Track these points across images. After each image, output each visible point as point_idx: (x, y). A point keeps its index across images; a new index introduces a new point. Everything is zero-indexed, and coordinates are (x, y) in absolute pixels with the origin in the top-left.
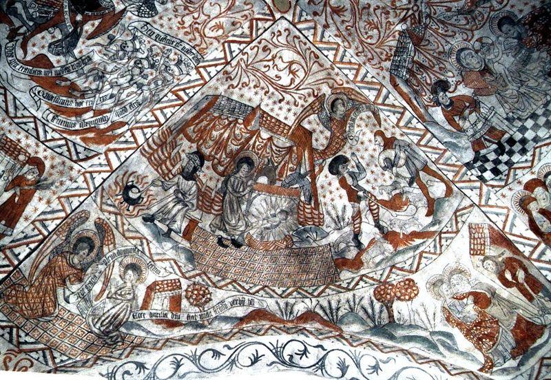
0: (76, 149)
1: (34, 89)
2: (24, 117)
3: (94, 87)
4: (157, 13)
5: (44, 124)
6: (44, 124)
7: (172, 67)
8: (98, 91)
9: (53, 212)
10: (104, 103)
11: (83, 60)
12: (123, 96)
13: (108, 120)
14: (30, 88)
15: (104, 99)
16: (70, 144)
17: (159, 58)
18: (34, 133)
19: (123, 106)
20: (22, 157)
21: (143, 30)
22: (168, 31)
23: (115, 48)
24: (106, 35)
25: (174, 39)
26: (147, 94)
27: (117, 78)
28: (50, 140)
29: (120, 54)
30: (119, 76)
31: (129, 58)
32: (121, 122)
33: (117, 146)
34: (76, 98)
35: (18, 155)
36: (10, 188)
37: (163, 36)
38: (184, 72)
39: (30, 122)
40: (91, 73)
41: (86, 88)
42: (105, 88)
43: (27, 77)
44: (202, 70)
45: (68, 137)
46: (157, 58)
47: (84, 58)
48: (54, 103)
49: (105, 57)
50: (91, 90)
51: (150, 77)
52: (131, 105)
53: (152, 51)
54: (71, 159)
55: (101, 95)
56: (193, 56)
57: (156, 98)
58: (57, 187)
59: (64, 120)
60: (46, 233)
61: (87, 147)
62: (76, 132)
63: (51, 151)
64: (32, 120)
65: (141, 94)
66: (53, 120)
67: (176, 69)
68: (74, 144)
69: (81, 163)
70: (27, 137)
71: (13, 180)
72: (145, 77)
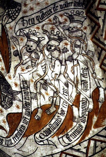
1: (37, 140)
3: (51, 94)
4: (20, 5)
5: (71, 148)
6: (71, 148)
7: (71, 25)
8: (56, 92)
10: (70, 94)
11: (24, 88)
12: (72, 77)
13: (87, 99)
14: (35, 142)
15: (67, 92)
16: (96, 138)
17: (56, 30)
19: (80, 81)
21: (26, 25)
22: (37, 9)
23: (26, 57)
24: (13, 56)
25: (49, 8)
26: (81, 58)
27: (53, 72)
29: (34, 57)
30: (52, 69)
31: (42, 52)
32: (94, 91)
34: (56, 112)
37: (40, 14)
38: (83, 20)
40: (38, 88)
41: (50, 100)
42: (56, 86)
43: (24, 139)
44: (100, 6)
45: (89, 136)
46: (55, 31)
47: (22, 86)
48: (55, 131)
49: (29, 70)
50: (53, 97)
51: (68, 47)
52: (83, 75)
53: (46, 31)
55: (62, 91)
56: (73, 4)
57: (91, 54)
59: (73, 131)
61: (104, 127)
62: (88, 128)
65: (78, 63)
66: (71, 141)
67: (75, 24)
72: (65, 50)
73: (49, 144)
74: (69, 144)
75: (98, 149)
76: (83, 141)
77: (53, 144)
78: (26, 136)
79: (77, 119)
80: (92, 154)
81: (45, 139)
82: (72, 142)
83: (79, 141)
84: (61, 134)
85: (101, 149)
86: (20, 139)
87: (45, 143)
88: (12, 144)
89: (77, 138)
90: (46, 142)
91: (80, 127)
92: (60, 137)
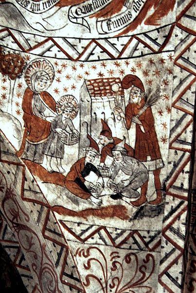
0: (150, 39)
1: (71, 14)
2: (86, 49)
6: (106, 39)
9: (179, 123)
14: (67, 17)
16: (142, 37)
18: (106, 56)
20: (115, 88)
28: (124, 50)
33: (181, 8)
35: (111, 89)
36: (129, 123)
39: (94, 49)
45: (135, 32)
48: (97, 10)
54: (155, 53)
58: (165, 90)
59: (119, 17)
60: (189, 147)
61: (158, 27)
62: (137, 21)
63: (132, 59)
64: (94, 44)
68: (145, 34)
69: (165, 49)
70: (104, 65)
71: (125, 115)
73: (82, 25)
74: (106, 33)
75: (137, 53)
76: (124, 35)
77: (88, 26)
78: (59, 6)
79: (130, 3)
80: (127, 57)
81: (80, 16)
82: (110, 31)
83: (119, 34)
84: (102, 16)
85: (140, 54)
86: (51, 7)
87: (78, 22)
88: (39, 10)
89: (119, 28)
90: (80, 21)
91: (129, 16)
92: (99, 19)
